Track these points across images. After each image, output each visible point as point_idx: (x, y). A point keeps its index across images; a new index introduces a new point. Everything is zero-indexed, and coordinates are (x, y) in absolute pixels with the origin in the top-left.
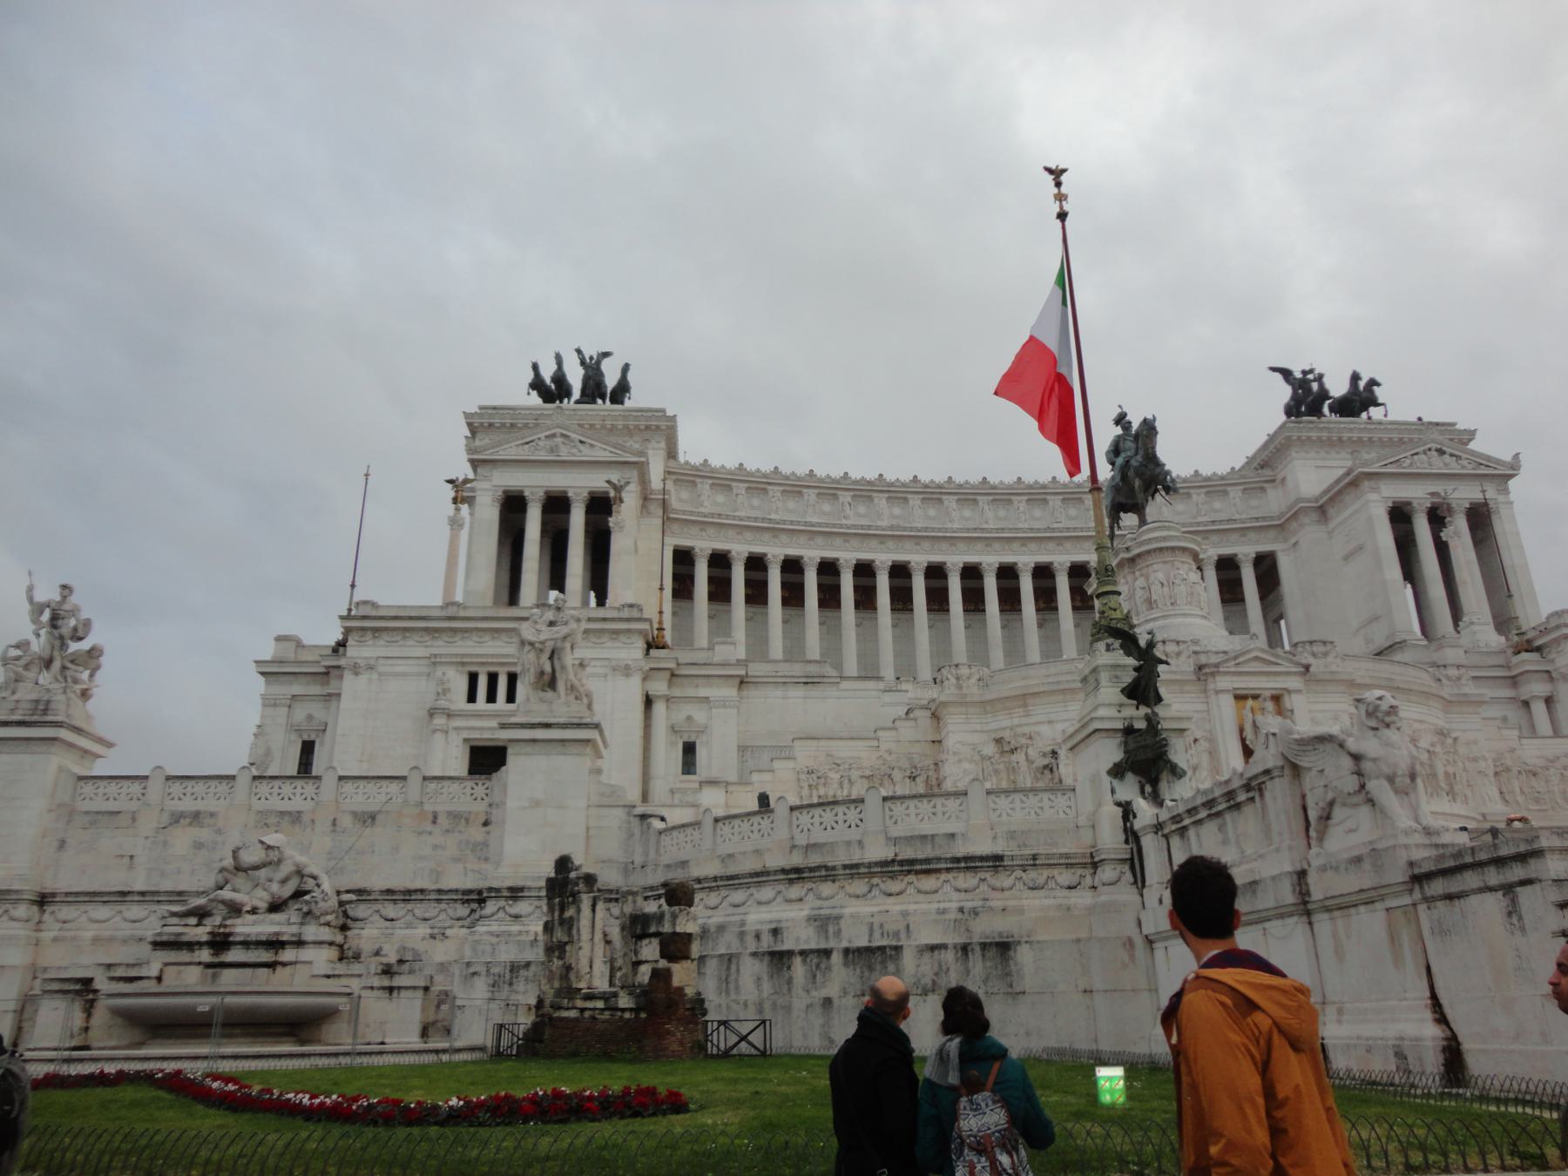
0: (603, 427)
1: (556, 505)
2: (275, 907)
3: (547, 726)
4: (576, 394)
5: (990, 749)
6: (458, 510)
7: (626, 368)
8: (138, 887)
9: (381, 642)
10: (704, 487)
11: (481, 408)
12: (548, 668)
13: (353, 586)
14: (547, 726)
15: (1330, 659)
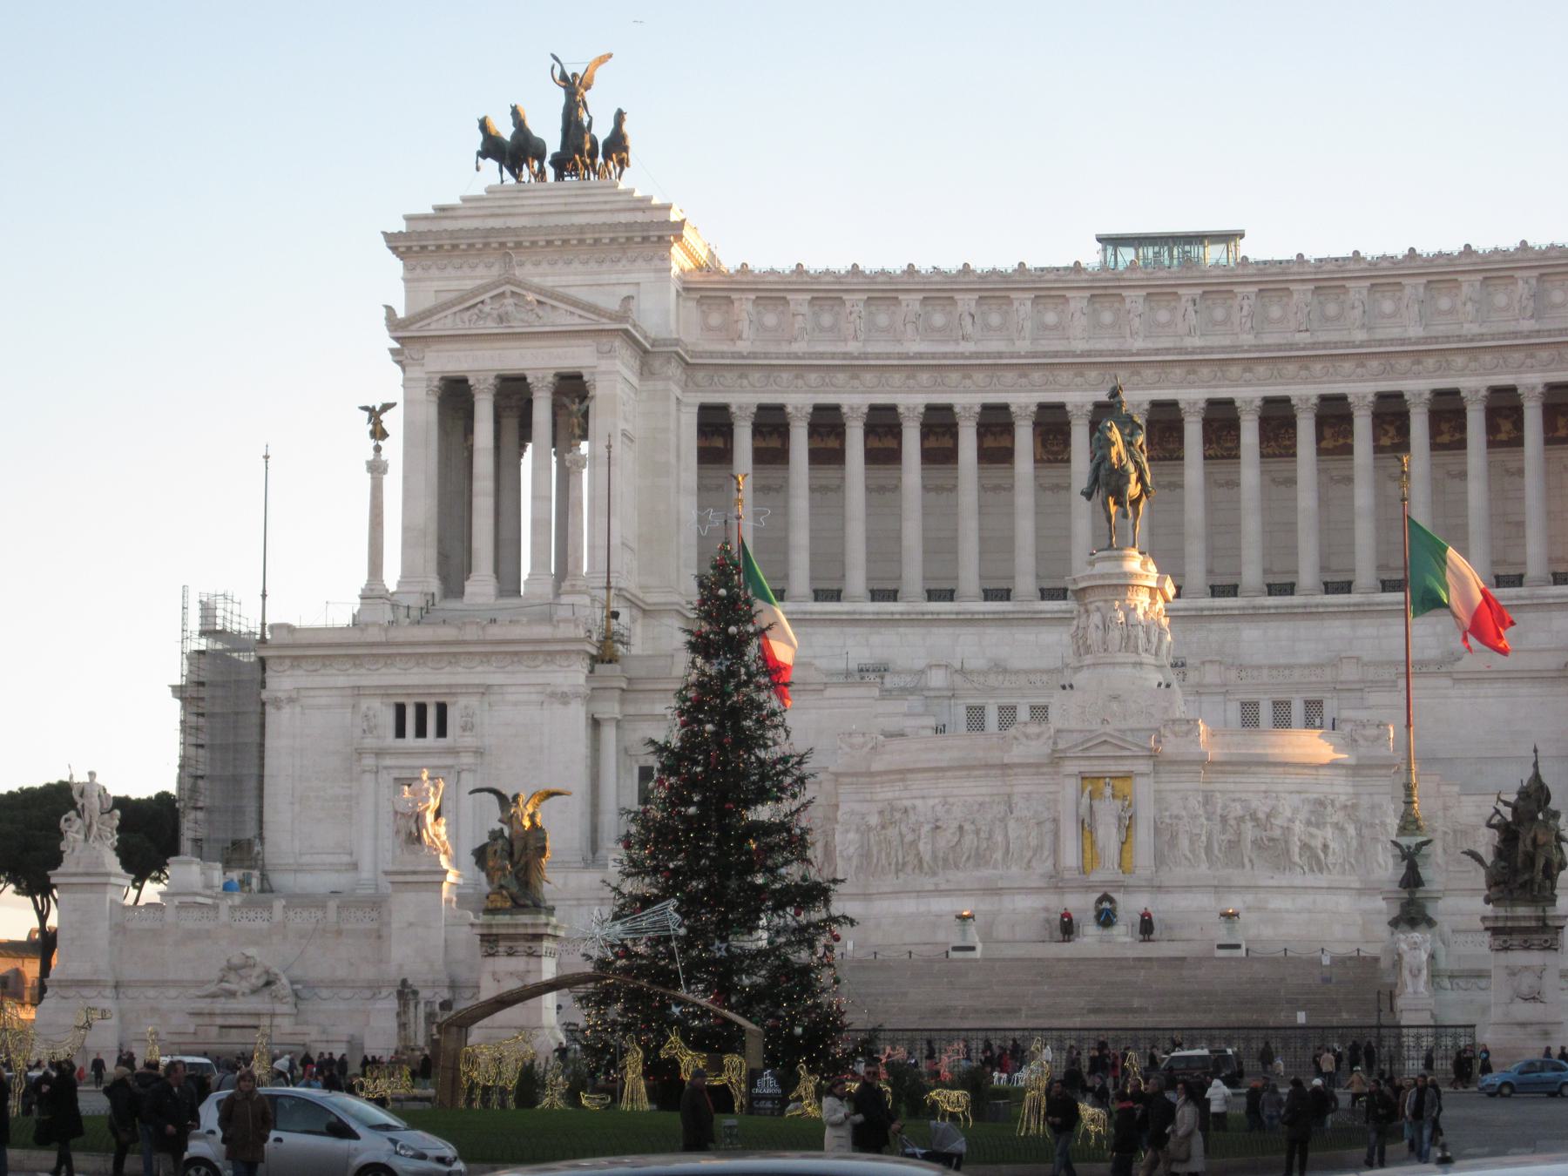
0: (581, 241)
1: (513, 394)
2: (254, 991)
3: (414, 873)
4: (553, 145)
5: (874, 820)
6: (378, 449)
7: (620, 117)
8: (171, 977)
9: (301, 672)
10: (744, 307)
11: (409, 218)
12: (414, 830)
13: (264, 596)
14: (414, 873)
15: (1191, 737)
